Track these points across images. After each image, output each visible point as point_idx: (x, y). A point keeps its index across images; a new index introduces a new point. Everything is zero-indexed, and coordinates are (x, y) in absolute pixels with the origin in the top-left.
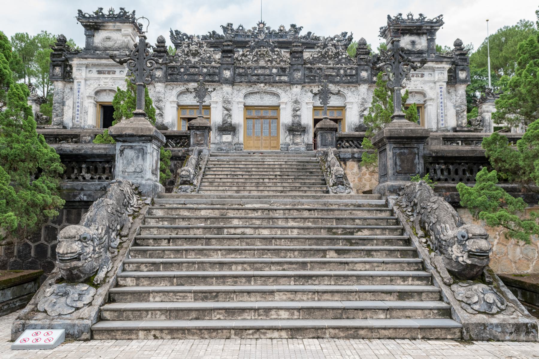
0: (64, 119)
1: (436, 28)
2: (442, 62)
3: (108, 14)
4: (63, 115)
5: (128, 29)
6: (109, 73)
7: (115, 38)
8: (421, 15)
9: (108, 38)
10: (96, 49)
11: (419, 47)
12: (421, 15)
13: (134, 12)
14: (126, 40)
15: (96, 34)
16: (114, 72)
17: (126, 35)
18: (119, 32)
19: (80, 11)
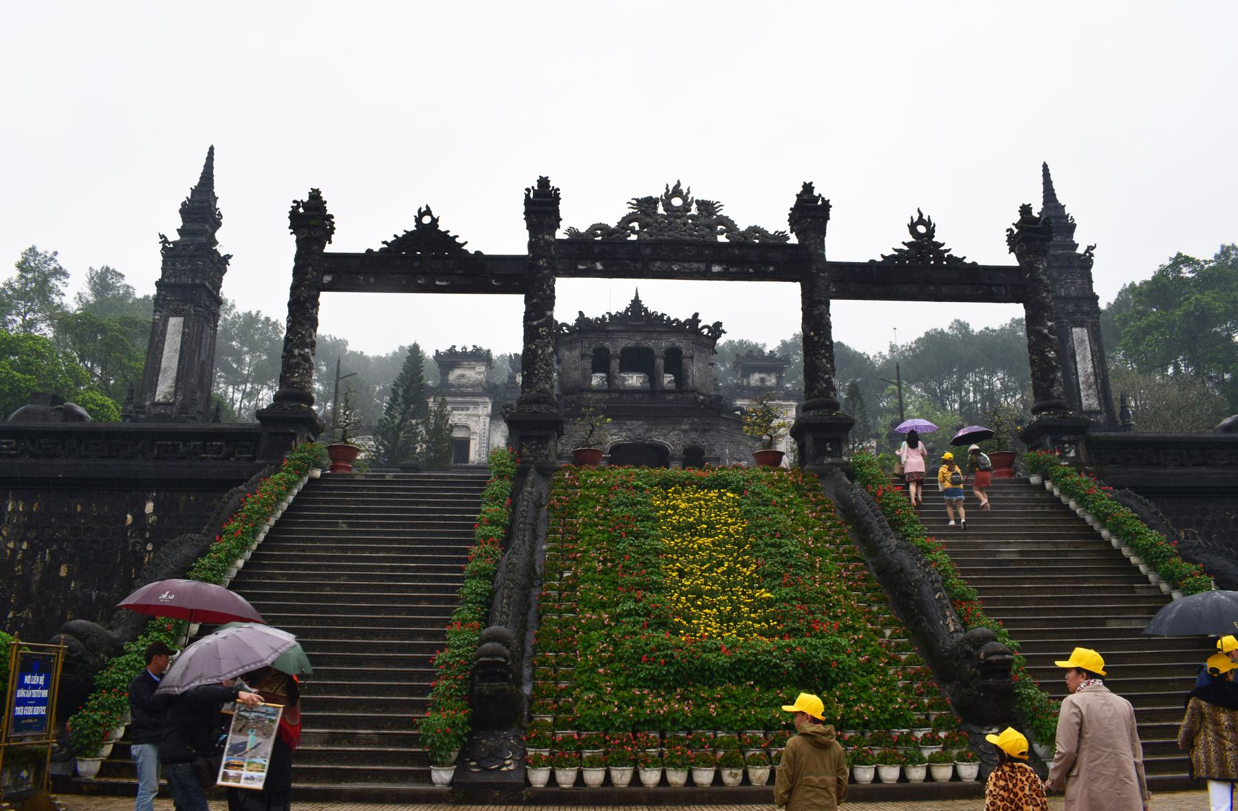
2: (789, 400)
6: (462, 410)
7: (469, 376)
9: (463, 376)
10: (452, 386)
11: (768, 384)
16: (468, 409)
17: (480, 373)
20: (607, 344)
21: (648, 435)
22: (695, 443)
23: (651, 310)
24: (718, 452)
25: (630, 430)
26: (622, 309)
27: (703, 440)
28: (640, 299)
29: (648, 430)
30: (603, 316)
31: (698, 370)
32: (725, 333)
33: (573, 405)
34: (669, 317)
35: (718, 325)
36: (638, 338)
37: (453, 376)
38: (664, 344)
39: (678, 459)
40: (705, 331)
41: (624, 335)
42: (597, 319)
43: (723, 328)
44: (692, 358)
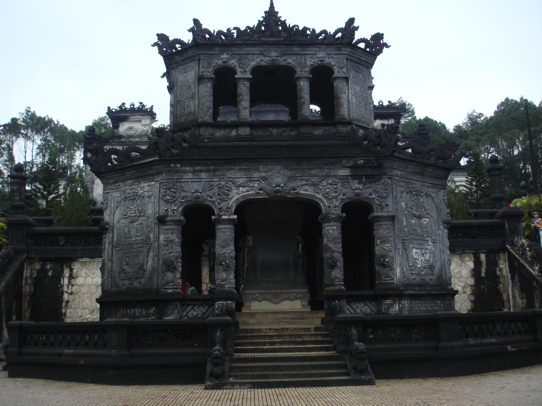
0: (94, 195)
1: (401, 113)
3: (129, 107)
4: (93, 192)
5: (146, 121)
7: (137, 128)
8: (389, 102)
9: (131, 128)
10: (121, 137)
12: (389, 102)
13: (152, 106)
14: (145, 129)
15: (121, 125)
17: (145, 125)
18: (139, 123)
19: (109, 108)
20: (233, 62)
21: (293, 185)
22: (357, 195)
23: (290, 23)
24: (390, 210)
25: (265, 179)
26: (253, 23)
27: (370, 190)
28: (276, 10)
29: (290, 178)
30: (229, 30)
31: (356, 94)
32: (387, 47)
33: (185, 145)
34: (314, 30)
35: (378, 37)
36: (274, 54)
37: (123, 128)
38: (310, 62)
39: (334, 220)
40: (362, 45)
41: (255, 50)
42: (220, 33)
43: (385, 40)
44: (347, 79)
